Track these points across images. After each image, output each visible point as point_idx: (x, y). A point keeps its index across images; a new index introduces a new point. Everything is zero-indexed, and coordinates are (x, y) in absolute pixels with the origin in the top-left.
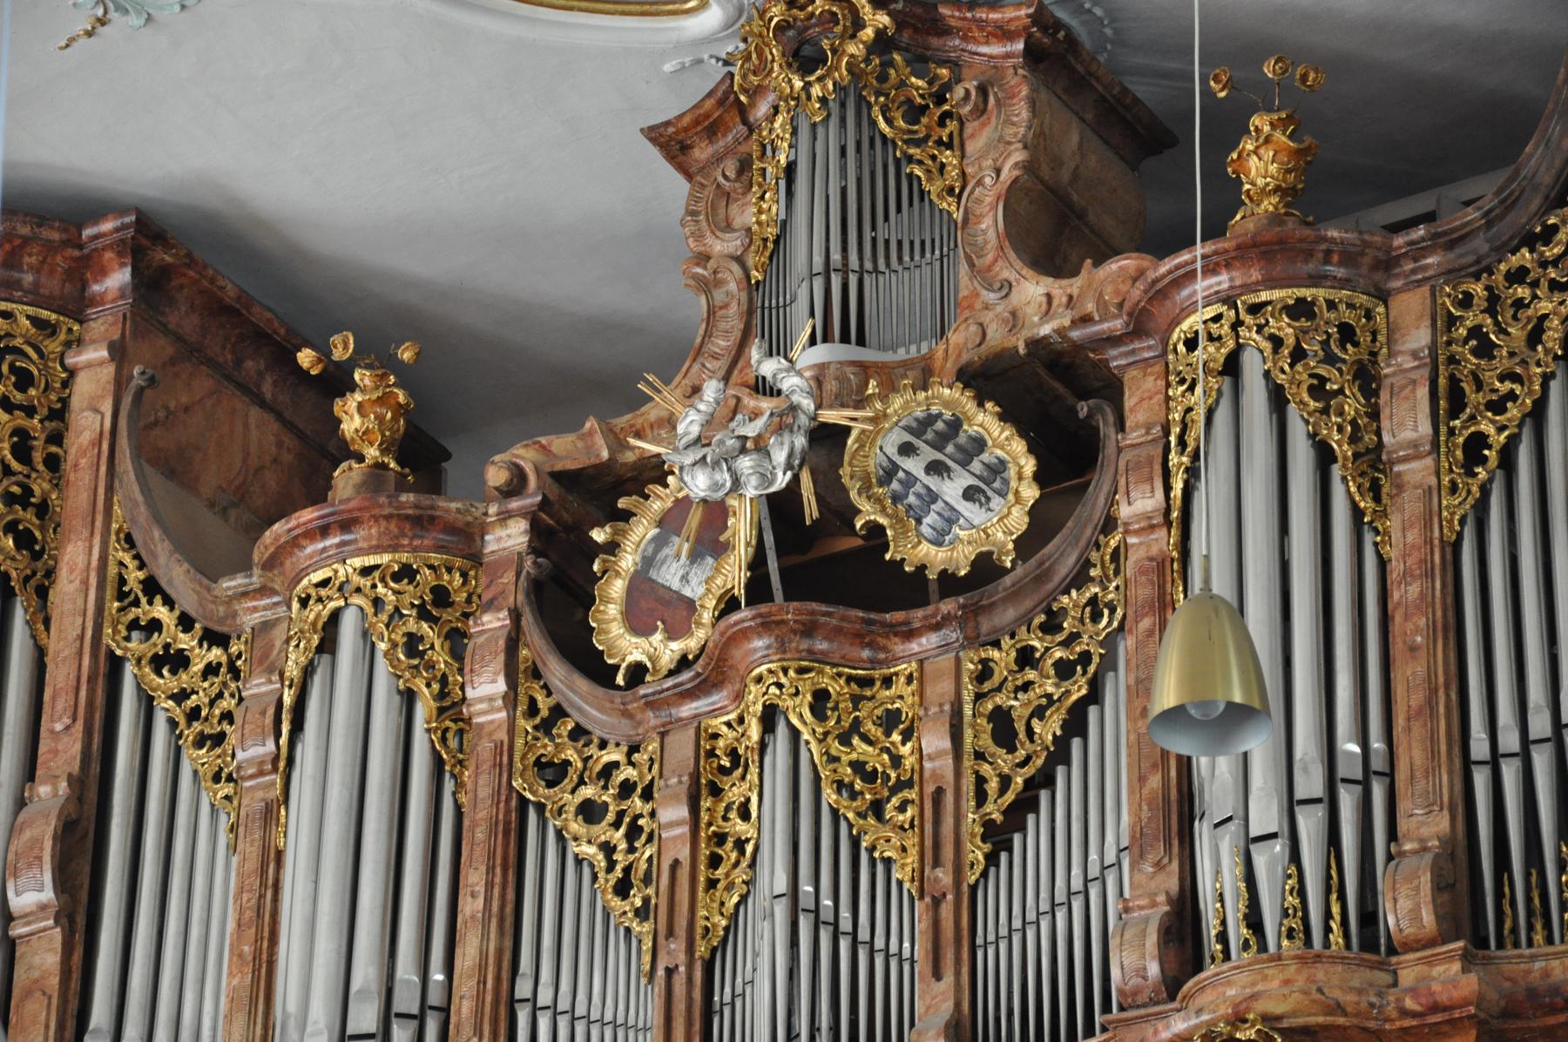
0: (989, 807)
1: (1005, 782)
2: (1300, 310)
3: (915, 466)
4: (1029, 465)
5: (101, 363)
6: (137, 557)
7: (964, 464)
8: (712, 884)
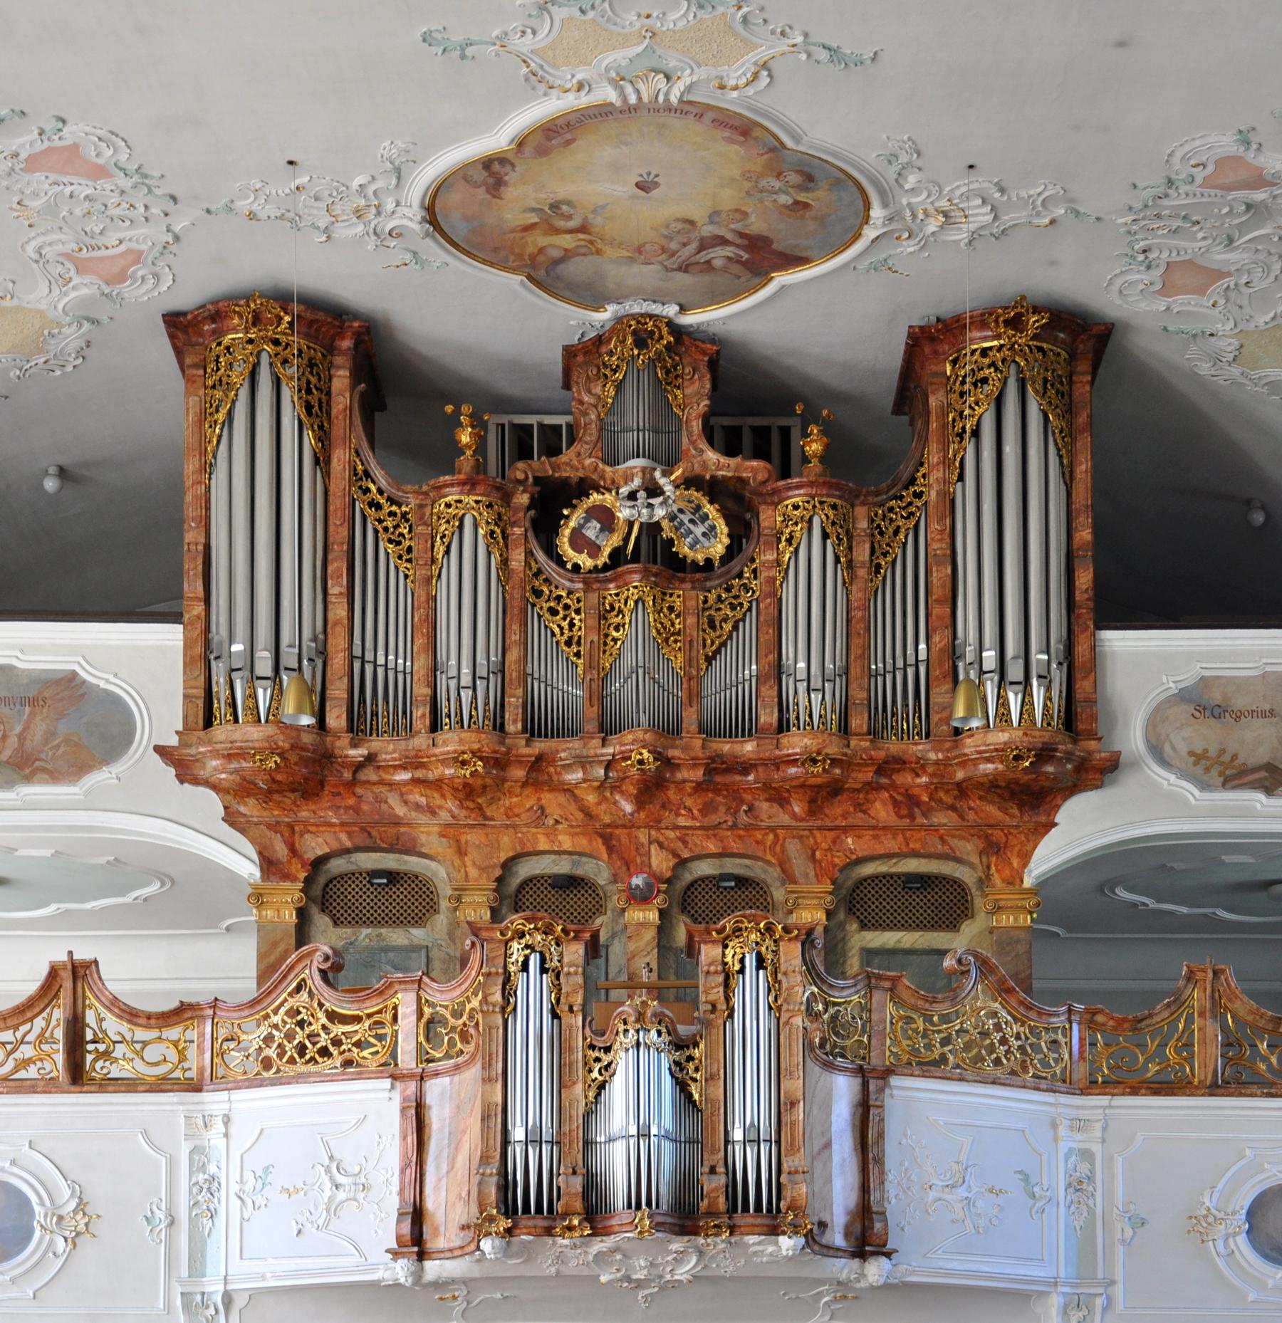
1: (713, 643)
2: (834, 507)
3: (685, 518)
4: (726, 530)
5: (345, 377)
6: (361, 460)
7: (703, 523)
8: (604, 652)
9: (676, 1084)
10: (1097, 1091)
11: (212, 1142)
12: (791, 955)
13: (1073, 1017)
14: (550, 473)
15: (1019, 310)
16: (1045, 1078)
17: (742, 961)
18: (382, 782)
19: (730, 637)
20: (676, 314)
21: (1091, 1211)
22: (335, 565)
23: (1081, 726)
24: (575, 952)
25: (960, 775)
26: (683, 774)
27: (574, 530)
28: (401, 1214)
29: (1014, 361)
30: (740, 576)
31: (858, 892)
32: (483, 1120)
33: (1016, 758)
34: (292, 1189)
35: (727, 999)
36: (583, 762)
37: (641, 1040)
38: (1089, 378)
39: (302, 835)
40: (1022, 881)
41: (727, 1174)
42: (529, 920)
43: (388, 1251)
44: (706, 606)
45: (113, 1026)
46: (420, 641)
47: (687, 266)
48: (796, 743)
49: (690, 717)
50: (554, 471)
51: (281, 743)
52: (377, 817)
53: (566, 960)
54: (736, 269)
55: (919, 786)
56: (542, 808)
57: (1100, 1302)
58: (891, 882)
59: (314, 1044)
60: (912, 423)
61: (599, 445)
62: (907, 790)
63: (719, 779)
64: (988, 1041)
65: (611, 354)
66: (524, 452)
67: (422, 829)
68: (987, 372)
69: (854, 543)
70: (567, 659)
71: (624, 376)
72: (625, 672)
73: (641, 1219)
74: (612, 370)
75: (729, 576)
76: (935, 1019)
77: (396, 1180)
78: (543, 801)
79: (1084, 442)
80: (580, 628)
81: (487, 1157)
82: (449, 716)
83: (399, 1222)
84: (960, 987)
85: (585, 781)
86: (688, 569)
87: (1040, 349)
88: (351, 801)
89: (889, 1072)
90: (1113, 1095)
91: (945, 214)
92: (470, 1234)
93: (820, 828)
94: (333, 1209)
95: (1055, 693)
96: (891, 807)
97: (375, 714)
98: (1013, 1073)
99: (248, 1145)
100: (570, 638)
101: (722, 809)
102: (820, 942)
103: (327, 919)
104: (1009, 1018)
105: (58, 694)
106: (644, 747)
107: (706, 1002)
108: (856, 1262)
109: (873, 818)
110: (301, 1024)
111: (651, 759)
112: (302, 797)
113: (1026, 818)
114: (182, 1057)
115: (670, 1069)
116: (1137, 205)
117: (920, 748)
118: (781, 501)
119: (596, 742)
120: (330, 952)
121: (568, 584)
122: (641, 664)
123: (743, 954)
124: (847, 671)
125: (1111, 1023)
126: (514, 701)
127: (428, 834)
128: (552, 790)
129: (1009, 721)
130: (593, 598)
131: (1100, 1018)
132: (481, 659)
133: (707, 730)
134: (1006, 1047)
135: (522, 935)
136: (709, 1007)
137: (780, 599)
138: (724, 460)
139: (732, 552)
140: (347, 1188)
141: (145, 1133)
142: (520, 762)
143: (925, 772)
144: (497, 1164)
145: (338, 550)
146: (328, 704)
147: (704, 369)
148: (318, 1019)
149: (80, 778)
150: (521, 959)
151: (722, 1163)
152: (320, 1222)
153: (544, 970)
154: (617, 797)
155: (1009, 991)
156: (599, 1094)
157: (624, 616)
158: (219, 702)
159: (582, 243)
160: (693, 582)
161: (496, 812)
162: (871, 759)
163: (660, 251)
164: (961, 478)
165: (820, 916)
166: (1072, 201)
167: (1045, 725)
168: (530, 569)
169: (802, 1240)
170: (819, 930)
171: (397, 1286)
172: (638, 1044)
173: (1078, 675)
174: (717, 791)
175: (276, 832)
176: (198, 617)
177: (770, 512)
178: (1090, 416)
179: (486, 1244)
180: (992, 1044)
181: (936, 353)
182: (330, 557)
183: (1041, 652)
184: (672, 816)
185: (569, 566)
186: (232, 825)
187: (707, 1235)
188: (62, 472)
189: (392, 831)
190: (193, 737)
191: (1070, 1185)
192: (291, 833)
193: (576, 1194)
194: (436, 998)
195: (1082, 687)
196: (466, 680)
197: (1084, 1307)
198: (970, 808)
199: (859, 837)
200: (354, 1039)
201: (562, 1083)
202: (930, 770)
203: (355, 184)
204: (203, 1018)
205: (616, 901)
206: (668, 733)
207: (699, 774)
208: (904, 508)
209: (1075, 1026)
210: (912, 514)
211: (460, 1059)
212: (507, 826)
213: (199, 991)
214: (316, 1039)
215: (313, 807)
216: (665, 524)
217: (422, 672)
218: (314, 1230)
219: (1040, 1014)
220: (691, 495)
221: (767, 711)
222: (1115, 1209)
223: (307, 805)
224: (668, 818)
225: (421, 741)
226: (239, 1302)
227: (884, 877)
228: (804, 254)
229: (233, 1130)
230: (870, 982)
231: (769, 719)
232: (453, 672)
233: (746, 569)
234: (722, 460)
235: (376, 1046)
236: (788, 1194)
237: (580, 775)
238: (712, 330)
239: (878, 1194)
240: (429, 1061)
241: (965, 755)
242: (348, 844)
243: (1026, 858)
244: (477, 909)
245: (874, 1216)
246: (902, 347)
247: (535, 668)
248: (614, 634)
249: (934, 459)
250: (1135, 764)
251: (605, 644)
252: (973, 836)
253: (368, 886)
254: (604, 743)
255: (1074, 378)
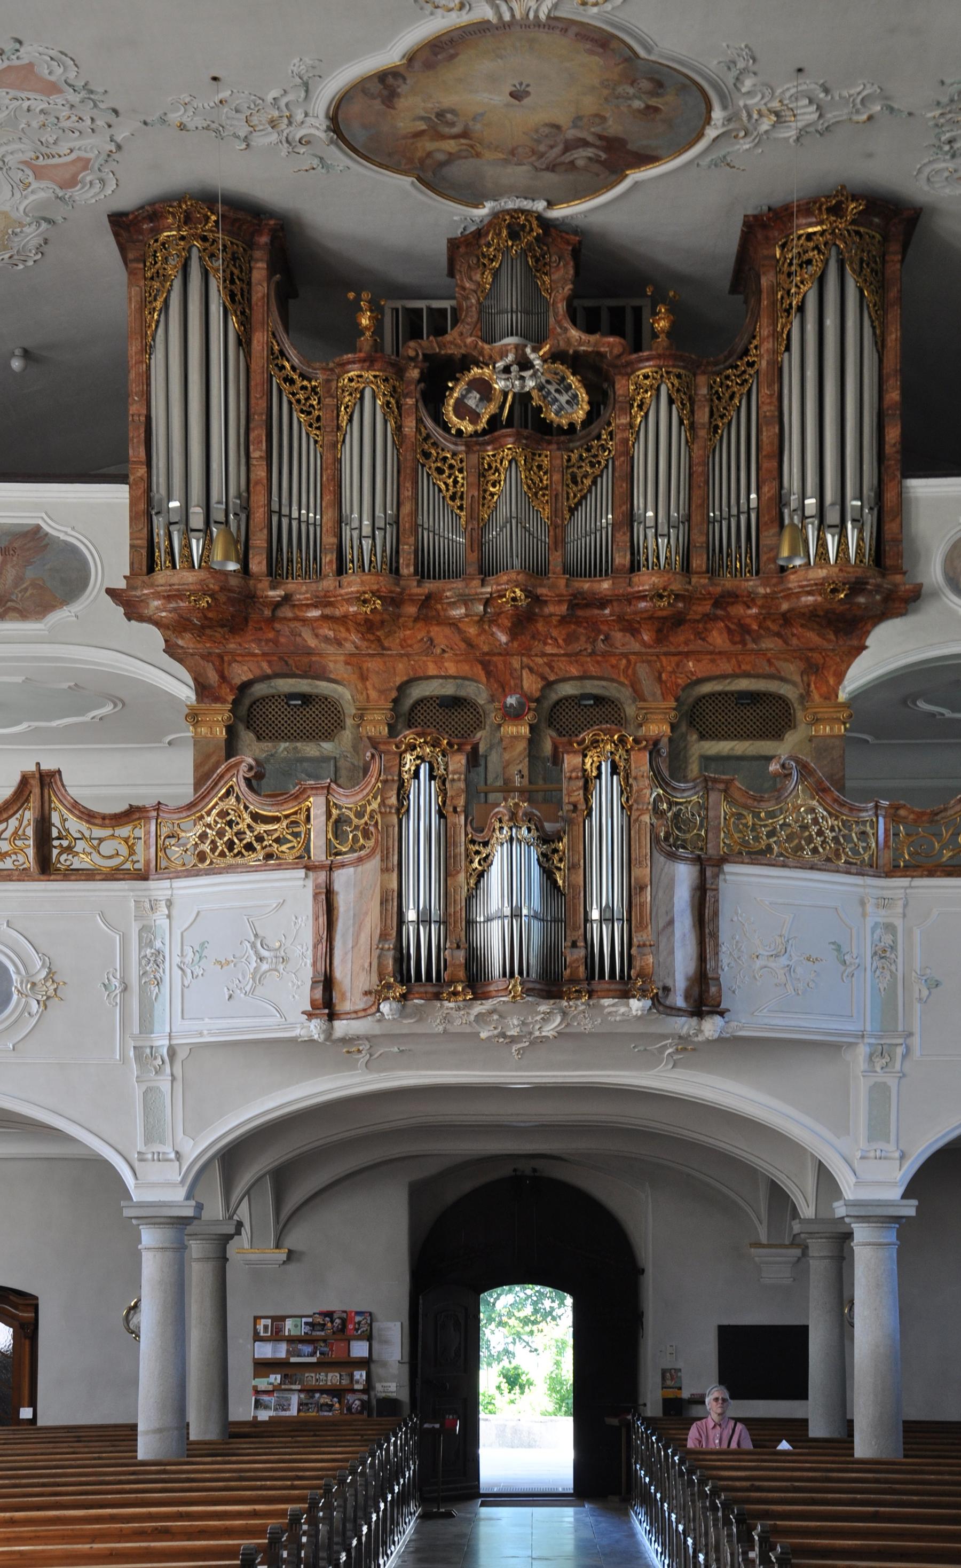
0: (571, 502)
1: (575, 496)
2: (679, 376)
3: (552, 388)
5: (262, 269)
6: (277, 342)
7: (567, 392)
8: (483, 505)
9: (544, 872)
10: (899, 874)
11: (158, 922)
12: (641, 763)
13: (879, 812)
14: (437, 350)
15: (840, 198)
16: (855, 864)
17: (599, 768)
18: (296, 619)
19: (590, 491)
20: (544, 209)
21: (893, 975)
22: (256, 432)
23: (889, 562)
24: (458, 762)
25: (785, 606)
26: (550, 609)
27: (457, 400)
28: (314, 983)
29: (835, 244)
30: (599, 437)
31: (698, 707)
32: (381, 903)
33: (834, 591)
34: (223, 961)
35: (587, 800)
36: (466, 600)
37: (514, 835)
38: (900, 257)
39: (230, 664)
40: (837, 696)
41: (586, 948)
42: (419, 735)
43: (303, 1013)
44: (570, 464)
45: (75, 825)
46: (327, 498)
47: (554, 166)
48: (646, 581)
49: (556, 561)
50: (440, 348)
51: (211, 586)
52: (292, 648)
53: (451, 768)
54: (596, 168)
55: (750, 616)
56: (431, 640)
57: (900, 1051)
58: (726, 698)
59: (241, 840)
60: (746, 302)
61: (479, 326)
62: (739, 620)
63: (580, 613)
64: (807, 834)
65: (489, 245)
66: (415, 333)
67: (331, 658)
68: (811, 254)
69: (696, 408)
70: (452, 511)
71: (500, 265)
72: (501, 521)
73: (514, 986)
74: (489, 259)
75: (589, 438)
76: (763, 815)
77: (310, 953)
78: (432, 634)
79: (894, 315)
80: (463, 485)
81: (386, 935)
82: (352, 562)
83: (312, 988)
84: (784, 788)
85: (467, 616)
86: (554, 432)
87: (858, 233)
88: (271, 635)
89: (723, 860)
90: (913, 877)
91: (777, 114)
92: (372, 999)
93: (666, 654)
94: (258, 978)
95: (867, 535)
96: (725, 635)
97: (290, 561)
98: (828, 860)
99: (186, 926)
100: (455, 493)
101: (583, 639)
102: (664, 751)
103: (251, 735)
104: (825, 813)
105: (25, 544)
106: (516, 586)
107: (569, 803)
108: (694, 1021)
109: (711, 645)
110: (230, 823)
111: (523, 597)
112: (230, 631)
113: (841, 643)
114: (132, 852)
115: (538, 860)
116: (945, 100)
117: (751, 584)
118: (633, 372)
119: (476, 582)
120: (253, 763)
121: (452, 447)
122: (514, 515)
123: (600, 763)
124: (689, 518)
125: (912, 816)
126: (407, 548)
127: (335, 662)
128: (439, 624)
129: (827, 559)
130: (474, 458)
131: (902, 812)
132: (379, 513)
133: (570, 571)
134: (822, 838)
135: (413, 748)
136: (571, 807)
137: (633, 458)
138: (584, 337)
139: (592, 417)
140: (270, 961)
141: (102, 915)
142: (412, 600)
143: (755, 604)
144: (394, 940)
145: (258, 419)
146: (251, 552)
147: (568, 257)
148: (244, 820)
149: (44, 616)
150: (413, 768)
151: (582, 938)
152: (248, 988)
153: (432, 777)
154: (494, 629)
155: (825, 790)
156: (478, 883)
157: (500, 474)
158: (160, 551)
159: (464, 147)
160: (558, 444)
161: (393, 643)
162: (709, 593)
163: (530, 154)
164: (788, 348)
165: (666, 728)
166: (887, 98)
167: (858, 562)
168: (421, 434)
169: (649, 1002)
170: (665, 741)
171: (312, 1041)
172: (511, 839)
173: (887, 518)
174: (578, 623)
175: (208, 661)
176: (141, 478)
177: (624, 382)
178: (900, 291)
179: (385, 1007)
180: (811, 835)
181: (767, 238)
182: (252, 425)
183: (855, 499)
184: (541, 645)
185: (453, 432)
186: (172, 655)
187: (569, 999)
188: (27, 354)
189: (305, 660)
190: (138, 581)
191: (875, 953)
192: (221, 662)
193: (460, 965)
194: (342, 801)
195: (890, 528)
196: (366, 531)
197: (887, 1056)
198: (793, 635)
199: (699, 661)
200: (274, 837)
201: (448, 872)
202: (759, 603)
203: (269, 98)
204: (148, 819)
205: (493, 717)
206: (537, 573)
207: (563, 609)
208: (739, 376)
209: (881, 820)
210: (746, 381)
211: (363, 853)
212: (402, 655)
213: (145, 796)
214: (243, 836)
215: (239, 640)
216: (535, 394)
217: (330, 524)
218: (242, 995)
219: (851, 810)
220: (556, 368)
221: (621, 554)
222: (914, 974)
223: (234, 638)
224: (537, 646)
225: (329, 583)
226: (181, 1055)
227: (720, 695)
228: (654, 153)
229: (175, 912)
230: (707, 785)
231: (622, 562)
232: (355, 524)
233: (603, 432)
234: (583, 337)
235: (290, 841)
236: (637, 964)
237: (463, 611)
238: (574, 223)
239: (713, 963)
240: (337, 854)
241: (790, 589)
242: (269, 671)
243: (840, 676)
244: (377, 726)
245: (710, 981)
246: (739, 234)
247: (425, 519)
248: (492, 489)
249: (765, 332)
250: (935, 594)
251: (484, 498)
252: (795, 658)
253: (286, 706)
254: (483, 585)
255: (887, 258)
